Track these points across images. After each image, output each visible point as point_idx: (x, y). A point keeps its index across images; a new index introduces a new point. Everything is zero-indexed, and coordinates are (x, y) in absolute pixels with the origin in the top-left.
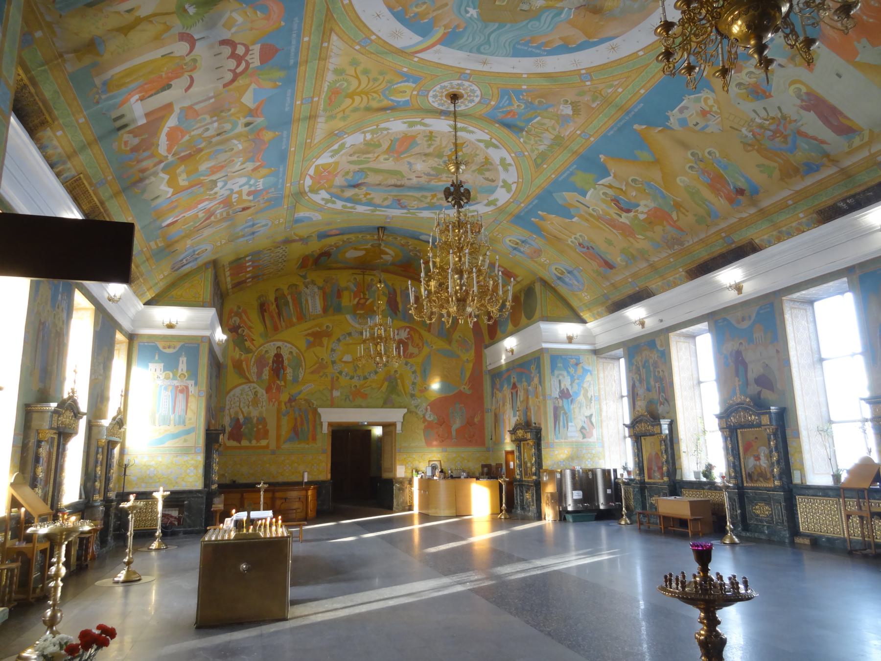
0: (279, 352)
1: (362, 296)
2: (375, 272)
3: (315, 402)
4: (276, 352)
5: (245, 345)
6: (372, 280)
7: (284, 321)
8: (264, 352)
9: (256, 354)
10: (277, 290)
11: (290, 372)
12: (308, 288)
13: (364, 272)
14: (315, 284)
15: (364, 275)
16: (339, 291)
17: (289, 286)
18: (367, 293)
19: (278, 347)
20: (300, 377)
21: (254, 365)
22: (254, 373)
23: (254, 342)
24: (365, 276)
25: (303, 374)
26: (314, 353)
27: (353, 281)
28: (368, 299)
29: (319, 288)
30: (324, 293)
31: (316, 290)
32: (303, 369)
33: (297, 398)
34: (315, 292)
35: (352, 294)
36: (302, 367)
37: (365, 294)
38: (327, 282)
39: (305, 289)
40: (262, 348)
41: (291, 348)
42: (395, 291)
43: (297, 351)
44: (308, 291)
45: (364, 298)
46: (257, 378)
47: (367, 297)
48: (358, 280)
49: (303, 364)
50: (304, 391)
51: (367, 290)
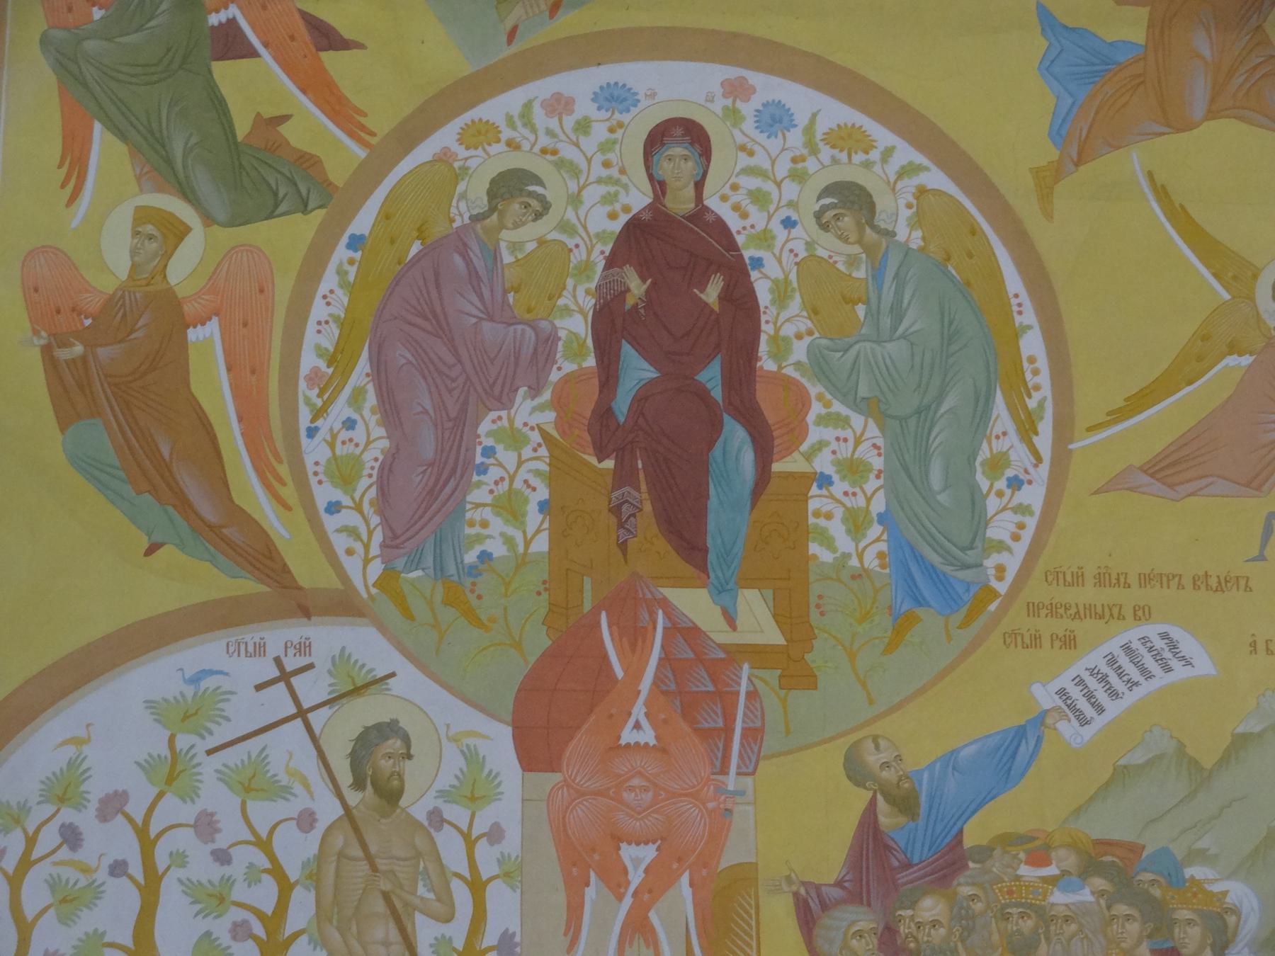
0: (680, 203)
3: (1238, 892)
4: (638, 198)
5: (218, 105)
8: (473, 195)
9: (363, 222)
11: (854, 469)
19: (657, 139)
20: (999, 529)
21: (340, 359)
22: (344, 473)
23: (332, 60)
25: (1034, 496)
26: (1162, 194)
32: (1027, 428)
33: (973, 835)
36: (1018, 387)
40: (445, 137)
41: (846, 139)
43: (936, 179)
46: (392, 543)
49: (1032, 345)
50: (1067, 728)
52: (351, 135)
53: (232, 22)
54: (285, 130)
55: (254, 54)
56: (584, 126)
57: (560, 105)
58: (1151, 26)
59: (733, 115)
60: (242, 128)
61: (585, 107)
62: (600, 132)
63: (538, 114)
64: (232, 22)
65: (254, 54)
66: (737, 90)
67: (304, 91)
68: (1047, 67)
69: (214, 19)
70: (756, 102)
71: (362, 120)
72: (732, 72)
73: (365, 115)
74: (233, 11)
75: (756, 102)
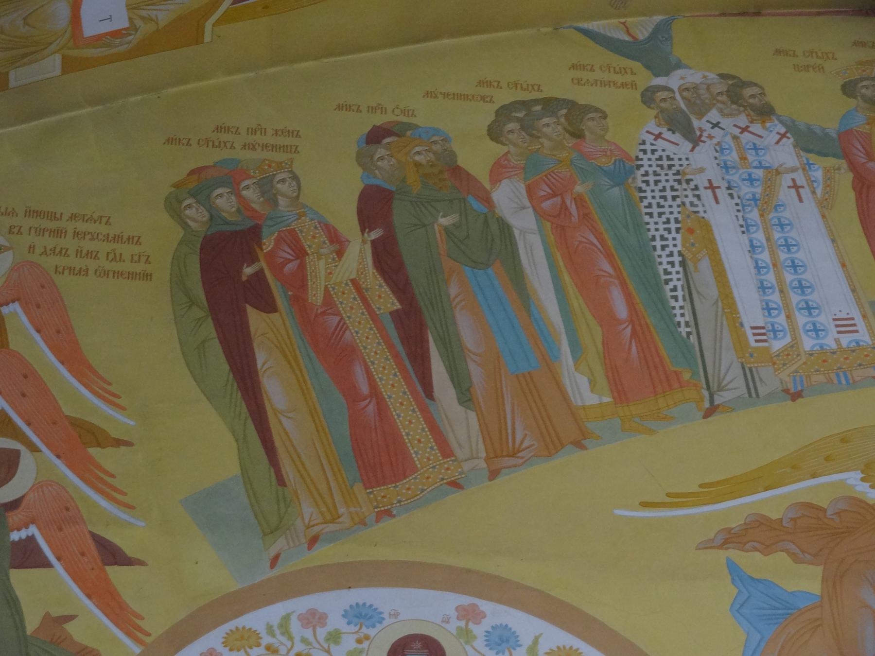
5: (13, 604)
7: (465, 397)
10: (376, 136)
12: (695, 141)
14: (765, 112)
17: (504, 113)
23: (116, 574)
34: (774, 173)
52: (129, 634)
53: (31, 539)
54: (71, 628)
55: (47, 565)
56: (335, 637)
57: (314, 619)
58: (824, 580)
59: (466, 635)
60: (32, 623)
61: (336, 621)
62: (349, 643)
63: (295, 626)
64: (31, 539)
65: (47, 565)
66: (470, 614)
67: (89, 596)
68: (737, 609)
69: (15, 536)
70: (486, 624)
71: (139, 622)
72: (465, 600)
73: (142, 618)
74: (33, 530)
75: (486, 624)
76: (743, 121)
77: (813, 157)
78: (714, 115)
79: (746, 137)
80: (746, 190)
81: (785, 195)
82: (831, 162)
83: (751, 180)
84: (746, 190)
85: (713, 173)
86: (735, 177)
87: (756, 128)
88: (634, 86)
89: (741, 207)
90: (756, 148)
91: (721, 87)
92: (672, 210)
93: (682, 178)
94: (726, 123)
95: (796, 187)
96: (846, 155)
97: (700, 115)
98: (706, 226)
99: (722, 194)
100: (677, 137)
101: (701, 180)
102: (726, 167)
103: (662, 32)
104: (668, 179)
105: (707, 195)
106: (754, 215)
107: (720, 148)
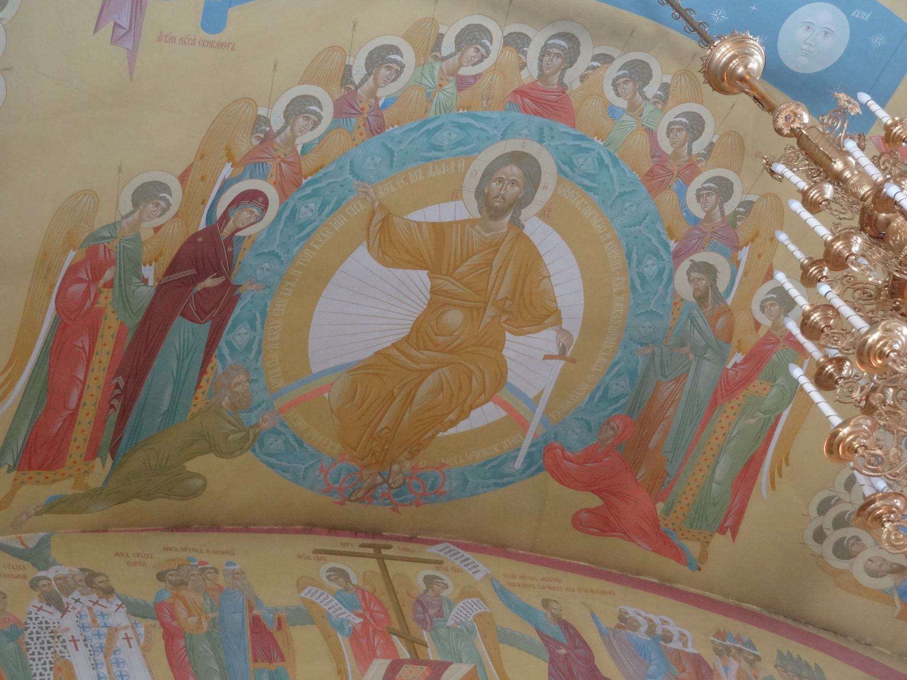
1: (404, 653)
2: (432, 551)
6: (429, 581)
12: (64, 610)
13: (377, 548)
14: (108, 592)
15: (381, 560)
16: (256, 624)
18: (426, 636)
24: (394, 567)
27: (336, 587)
28: (445, 665)
29: (135, 610)
30: (170, 636)
31: (120, 618)
34: (113, 630)
35: (344, 643)
37: (413, 643)
38: (180, 584)
39: (51, 615)
42: (566, 626)
44: (69, 621)
45: (416, 661)
47: (432, 654)
48: (354, 579)
51: (423, 623)
76: (94, 597)
77: (138, 619)
78: (76, 594)
79: (96, 608)
80: (96, 642)
81: (120, 643)
82: (150, 622)
83: (99, 635)
84: (96, 642)
85: (75, 631)
86: (89, 633)
87: (103, 602)
88: (25, 577)
89: (93, 652)
90: (102, 615)
91: (81, 576)
92: (48, 656)
93: (54, 635)
94: (84, 599)
95: (127, 638)
96: (159, 618)
97: (67, 594)
98: (69, 666)
99: (80, 644)
100: (52, 609)
101: (67, 636)
102: (83, 627)
103: (44, 543)
104: (45, 636)
105: (71, 646)
106: (100, 657)
107: (80, 615)
